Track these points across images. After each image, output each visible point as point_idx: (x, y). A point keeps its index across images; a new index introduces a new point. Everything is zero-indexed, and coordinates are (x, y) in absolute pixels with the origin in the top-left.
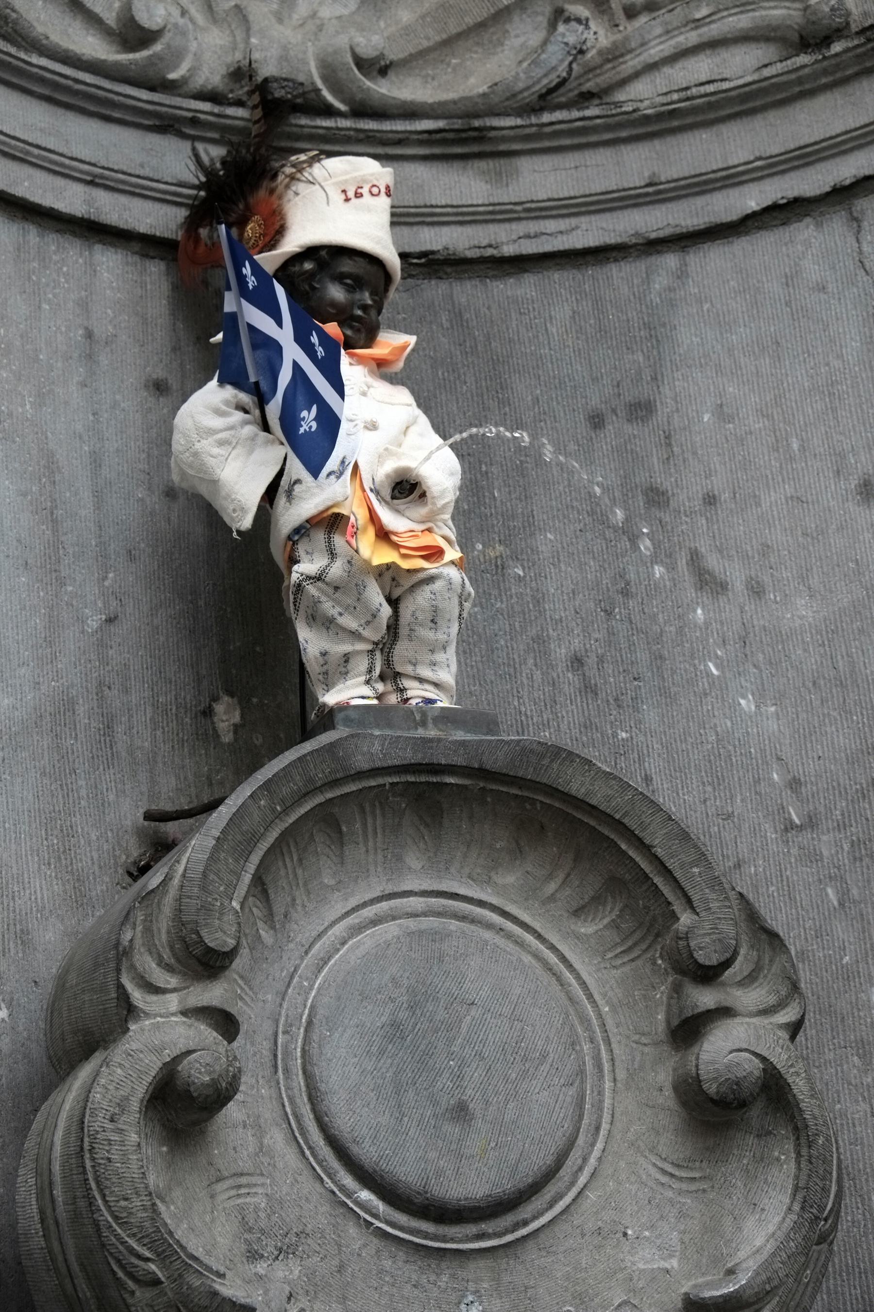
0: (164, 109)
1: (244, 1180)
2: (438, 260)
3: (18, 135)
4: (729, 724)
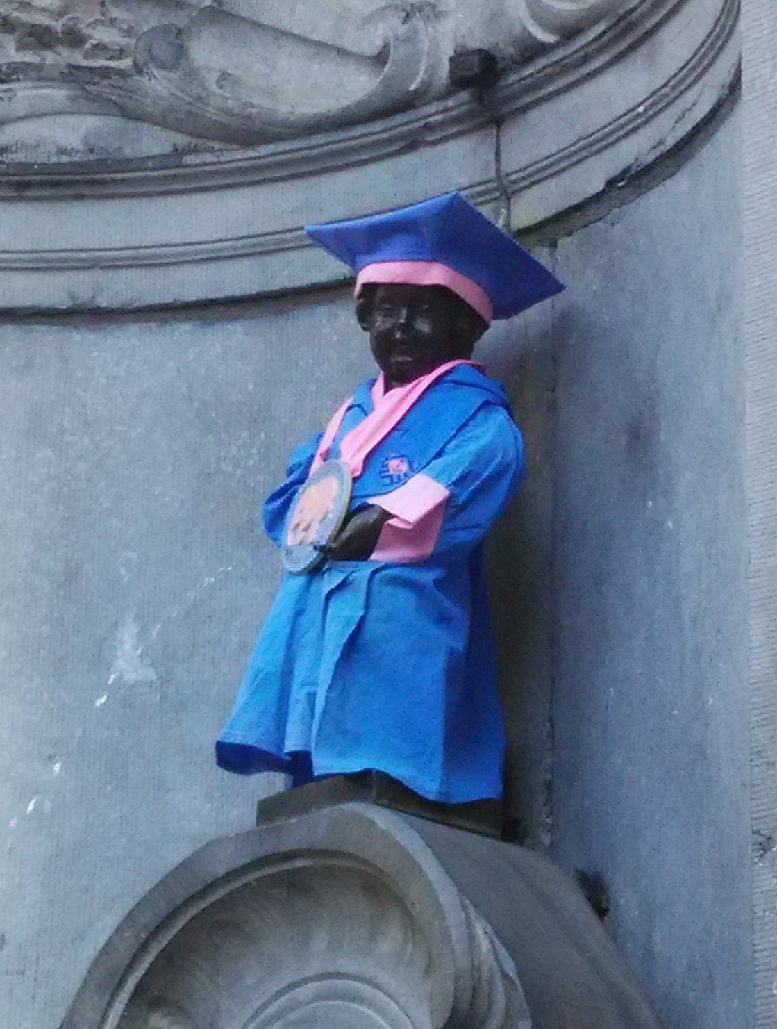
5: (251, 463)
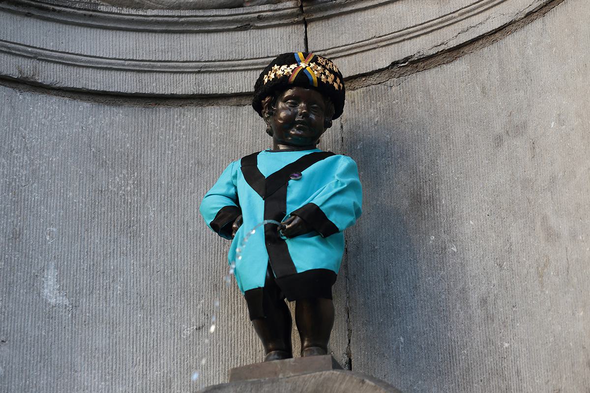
0: (240, 17)
2: (414, 61)
3: (144, 59)
4: (560, 328)
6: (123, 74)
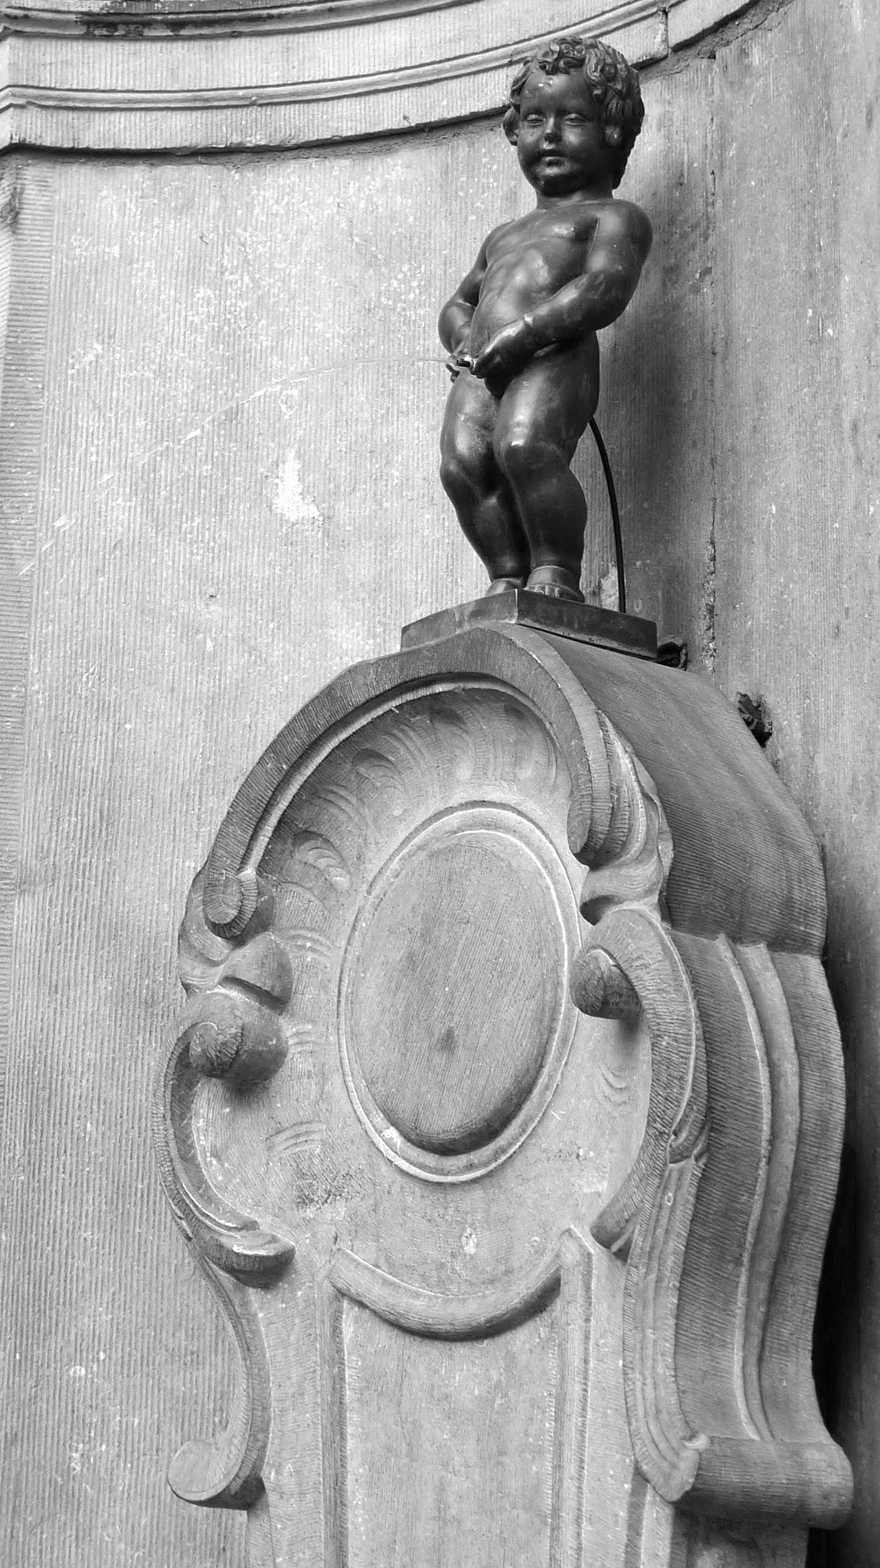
1: (304, 1128)
5: (412, 296)
6: (396, 94)
